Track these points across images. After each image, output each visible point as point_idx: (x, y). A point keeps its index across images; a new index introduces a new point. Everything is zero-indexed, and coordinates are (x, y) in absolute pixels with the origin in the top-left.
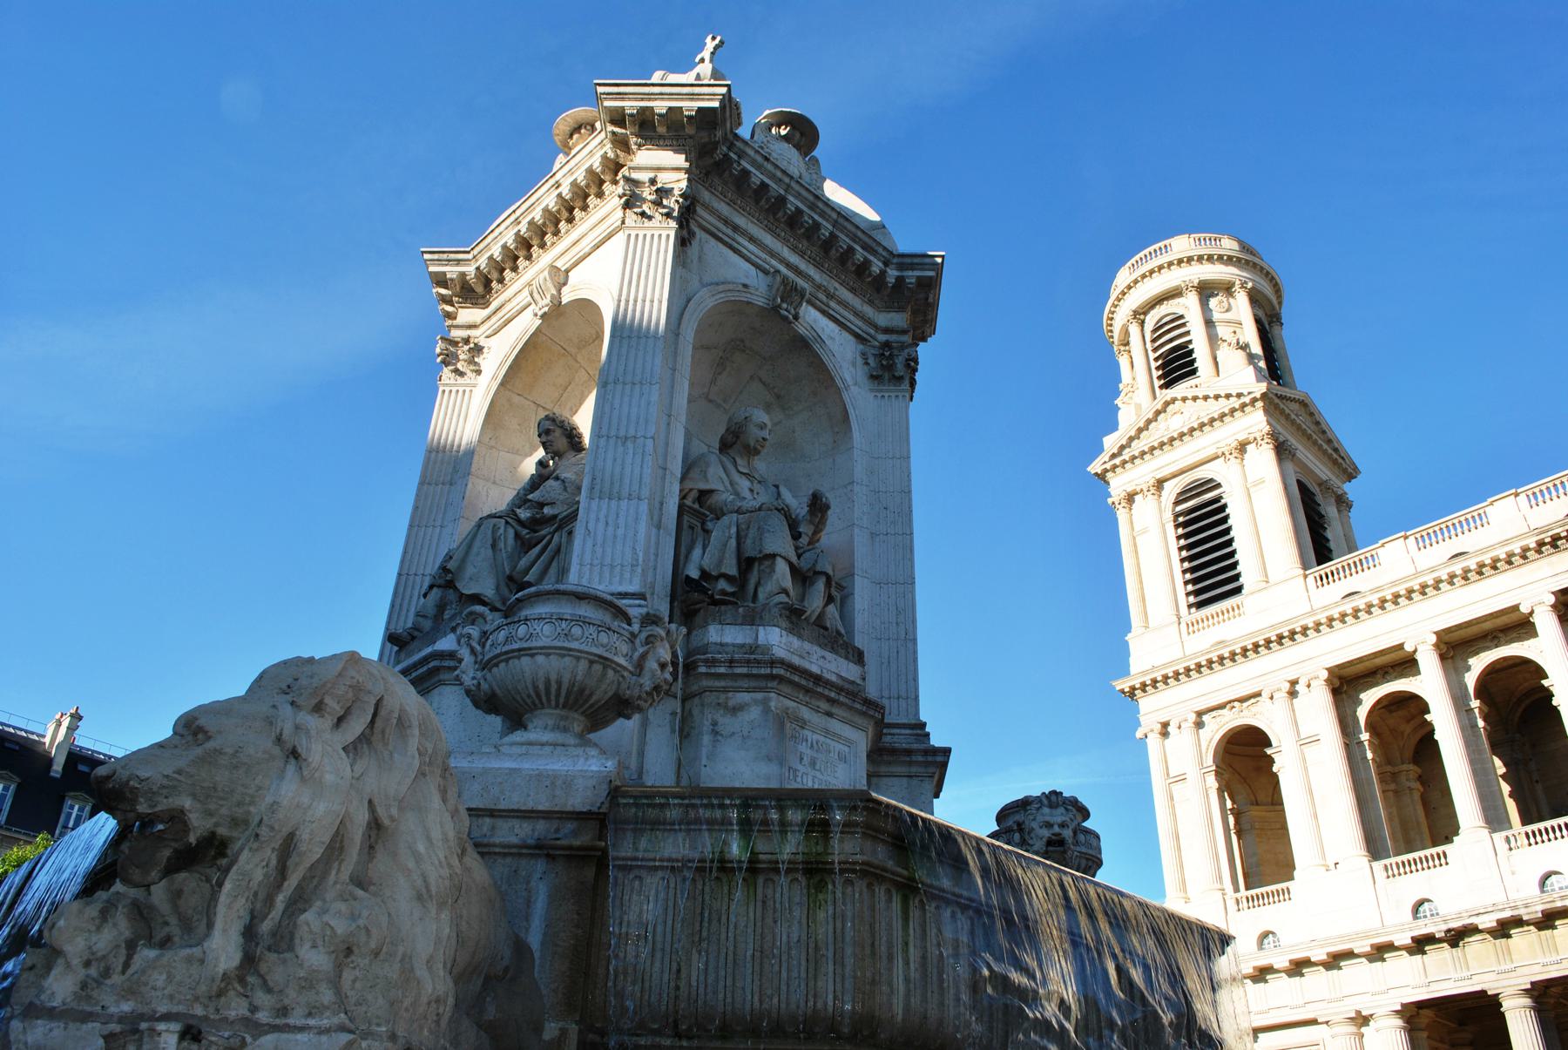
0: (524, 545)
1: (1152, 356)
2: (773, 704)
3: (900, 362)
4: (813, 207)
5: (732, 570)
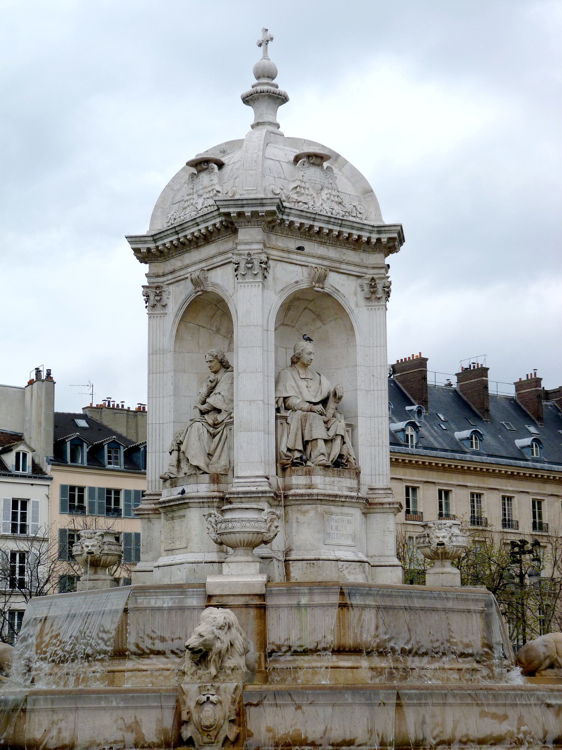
0: (213, 436)
2: (319, 509)
3: (380, 287)
4: (328, 222)
5: (301, 448)
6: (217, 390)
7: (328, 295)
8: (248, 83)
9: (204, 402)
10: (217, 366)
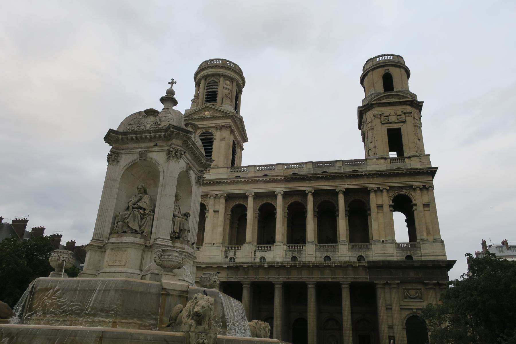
0: (142, 219)
1: (206, 91)
5: (178, 231)
6: (143, 200)
7: (188, 177)
8: (164, 94)
9: (134, 205)
10: (142, 190)
